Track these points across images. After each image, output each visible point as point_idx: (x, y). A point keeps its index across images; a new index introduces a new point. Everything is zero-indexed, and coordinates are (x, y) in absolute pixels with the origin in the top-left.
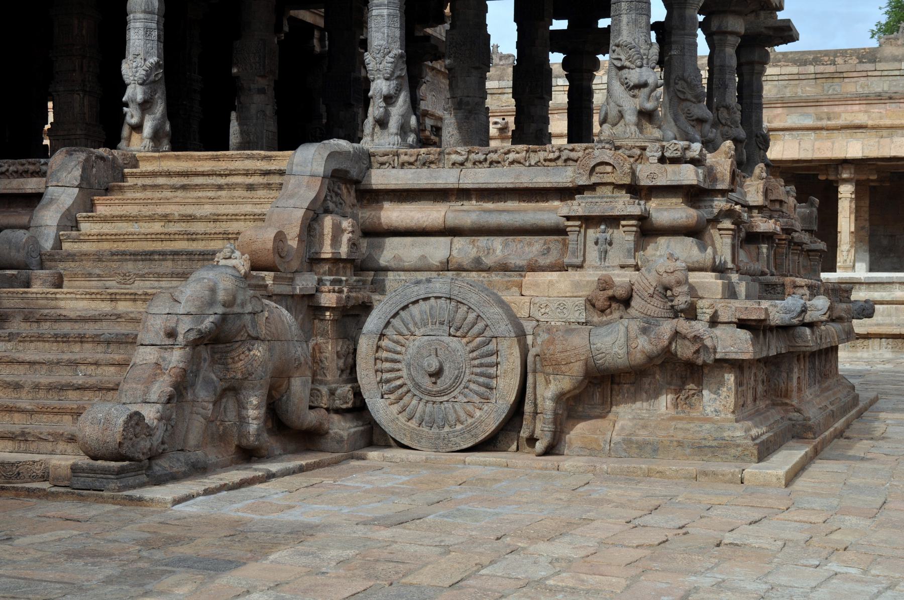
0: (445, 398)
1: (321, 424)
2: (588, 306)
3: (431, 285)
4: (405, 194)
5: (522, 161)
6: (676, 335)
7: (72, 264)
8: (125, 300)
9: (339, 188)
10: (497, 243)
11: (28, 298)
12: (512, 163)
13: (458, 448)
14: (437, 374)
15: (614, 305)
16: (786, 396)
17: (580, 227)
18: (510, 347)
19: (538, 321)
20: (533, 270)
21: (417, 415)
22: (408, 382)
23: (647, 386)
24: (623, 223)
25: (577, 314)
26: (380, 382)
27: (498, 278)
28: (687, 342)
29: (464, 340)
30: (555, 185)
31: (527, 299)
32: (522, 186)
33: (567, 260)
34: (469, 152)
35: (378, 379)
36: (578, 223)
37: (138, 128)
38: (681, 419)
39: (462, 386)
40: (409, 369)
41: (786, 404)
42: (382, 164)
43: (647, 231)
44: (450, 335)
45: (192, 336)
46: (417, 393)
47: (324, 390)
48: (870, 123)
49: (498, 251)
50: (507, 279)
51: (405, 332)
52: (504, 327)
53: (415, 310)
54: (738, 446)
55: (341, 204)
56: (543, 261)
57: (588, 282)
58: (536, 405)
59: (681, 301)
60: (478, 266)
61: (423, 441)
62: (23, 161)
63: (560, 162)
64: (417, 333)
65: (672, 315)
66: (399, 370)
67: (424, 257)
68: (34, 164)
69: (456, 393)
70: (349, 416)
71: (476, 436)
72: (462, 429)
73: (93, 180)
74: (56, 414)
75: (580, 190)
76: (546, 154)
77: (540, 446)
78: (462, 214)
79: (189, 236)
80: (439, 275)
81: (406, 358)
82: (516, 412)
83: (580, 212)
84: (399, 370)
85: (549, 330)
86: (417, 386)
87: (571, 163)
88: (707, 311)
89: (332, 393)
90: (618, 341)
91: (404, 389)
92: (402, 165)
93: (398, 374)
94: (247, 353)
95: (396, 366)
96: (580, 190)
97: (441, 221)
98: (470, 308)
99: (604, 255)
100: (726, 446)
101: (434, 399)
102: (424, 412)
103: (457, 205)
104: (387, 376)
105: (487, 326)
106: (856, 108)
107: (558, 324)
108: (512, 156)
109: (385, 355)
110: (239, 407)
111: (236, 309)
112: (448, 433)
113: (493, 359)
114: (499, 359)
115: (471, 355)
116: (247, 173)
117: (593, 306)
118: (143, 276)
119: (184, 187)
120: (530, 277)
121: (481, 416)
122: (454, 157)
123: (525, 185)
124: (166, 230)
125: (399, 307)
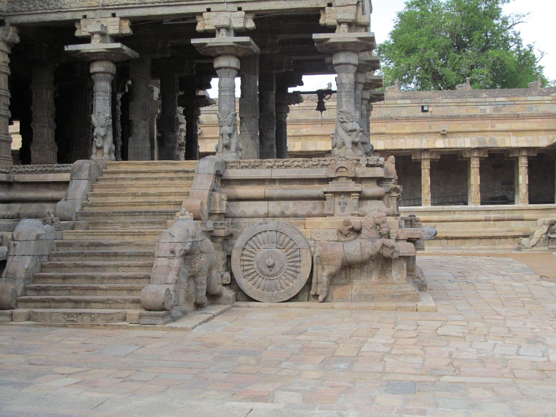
0: (276, 278)
1: (221, 291)
2: (339, 233)
3: (268, 225)
6: (384, 245)
7: (92, 218)
8: (129, 235)
10: (290, 203)
11: (78, 235)
12: (296, 167)
15: (351, 233)
16: (412, 271)
18: (306, 253)
20: (309, 217)
21: (262, 286)
22: (257, 270)
23: (366, 269)
24: (352, 194)
26: (243, 270)
27: (293, 221)
28: (388, 249)
29: (284, 250)
30: (318, 177)
31: (309, 230)
33: (326, 212)
34: (275, 161)
36: (331, 195)
37: (100, 148)
38: (383, 284)
41: (413, 275)
42: (232, 167)
43: (363, 198)
45: (182, 252)
46: (262, 275)
48: (387, 132)
49: (291, 208)
50: (298, 221)
51: (255, 247)
53: (259, 236)
54: (410, 295)
57: (337, 222)
58: (317, 279)
59: (384, 231)
60: (283, 215)
62: (45, 165)
63: (319, 166)
65: (379, 237)
67: (256, 211)
68: (50, 167)
69: (281, 275)
71: (290, 294)
74: (119, 290)
75: (331, 179)
77: (321, 298)
82: (309, 283)
83: (333, 190)
86: (262, 272)
87: (324, 166)
89: (222, 276)
90: (354, 249)
91: (255, 274)
92: (242, 167)
93: (252, 267)
95: (251, 263)
96: (331, 179)
97: (263, 194)
98: (287, 235)
99: (343, 209)
100: (405, 295)
101: (270, 278)
103: (270, 187)
104: (246, 268)
105: (295, 243)
106: (380, 124)
108: (296, 163)
109: (245, 258)
110: (196, 284)
111: (196, 239)
113: (298, 259)
115: (287, 257)
116: (167, 172)
117: (342, 233)
118: (133, 223)
120: (308, 220)
122: (268, 164)
124: (135, 201)
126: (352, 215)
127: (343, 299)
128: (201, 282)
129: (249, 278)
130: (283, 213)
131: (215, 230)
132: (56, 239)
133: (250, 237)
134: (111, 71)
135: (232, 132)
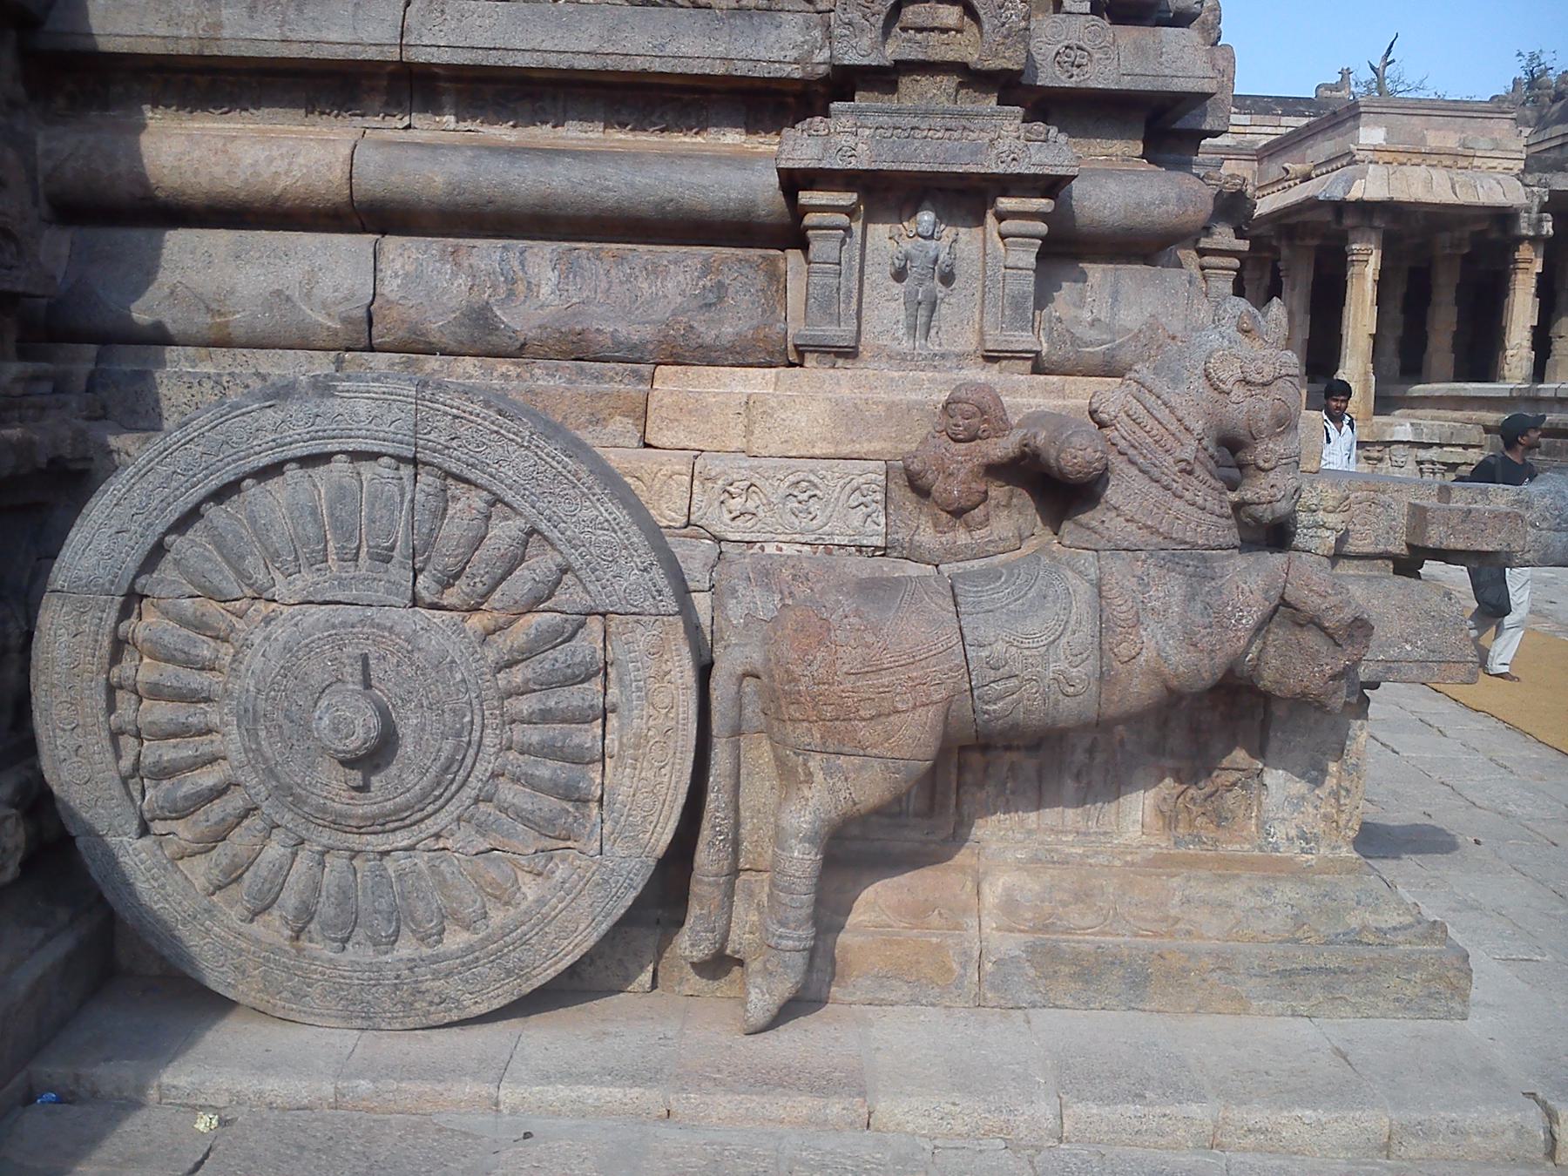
0: (402, 839)
2: (901, 493)
10: (541, 260)
14: (376, 755)
15: (998, 492)
17: (850, 212)
18: (657, 652)
19: (718, 540)
21: (290, 899)
24: (1005, 203)
25: (856, 518)
32: (625, 65)
36: (848, 198)
38: (1192, 863)
39: (468, 793)
40: (253, 734)
50: (589, 386)
52: (634, 577)
57: (890, 407)
61: (315, 991)
69: (443, 818)
72: (470, 949)
75: (844, 83)
78: (413, 153)
80: (339, 364)
81: (234, 686)
83: (863, 160)
85: (766, 575)
88: (1331, 519)
91: (234, 802)
93: (205, 746)
96: (844, 83)
98: (497, 500)
99: (924, 314)
101: (355, 841)
102: (316, 888)
103: (390, 127)
107: (788, 550)
120: (670, 383)
121: (541, 902)
123: (639, 64)
126: (991, 358)
127: (923, 979)
129: (184, 831)
130: (481, 318)
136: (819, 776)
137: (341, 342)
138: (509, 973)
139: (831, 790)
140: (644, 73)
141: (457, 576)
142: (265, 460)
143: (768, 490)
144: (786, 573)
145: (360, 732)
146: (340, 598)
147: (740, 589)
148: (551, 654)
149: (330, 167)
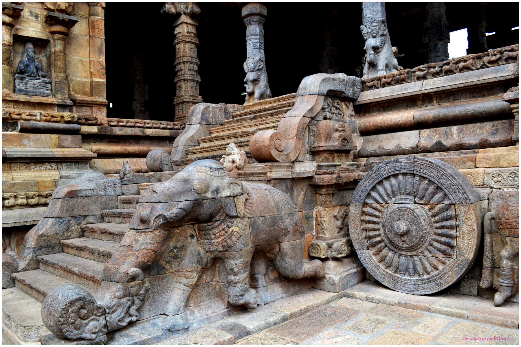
0: (414, 253)
3: (398, 164)
4: (387, 105)
5: (470, 66)
9: (338, 105)
10: (455, 129)
13: (427, 293)
19: (492, 188)
20: (484, 147)
22: (385, 239)
26: (365, 237)
29: (427, 207)
31: (481, 170)
34: (429, 68)
35: (364, 236)
37: (252, 94)
39: (427, 244)
40: (385, 230)
44: (415, 203)
46: (392, 248)
47: (323, 244)
49: (455, 136)
51: (381, 201)
53: (386, 184)
55: (340, 114)
56: (492, 139)
60: (439, 148)
64: (389, 202)
66: (379, 230)
67: (398, 146)
69: (422, 249)
70: (346, 260)
72: (429, 278)
73: (210, 120)
76: (488, 58)
77: (498, 297)
79: (240, 144)
84: (379, 230)
86: (391, 242)
87: (510, 61)
89: (330, 246)
94: (226, 229)
102: (399, 263)
109: (367, 218)
112: (417, 280)
113: (453, 222)
114: (457, 223)
115: (433, 219)
119: (254, 118)
120: (482, 153)
121: (444, 269)
122: (419, 73)
125: (375, 183)
128: (232, 270)
130: (439, 143)
131: (316, 176)
132: (123, 194)
133: (372, 185)
134: (258, 12)
135: (379, 44)
136: (509, 243)
137: (411, 152)
138: (437, 284)
139: (513, 246)
140: (475, 85)
141: (423, 197)
142: (386, 176)
143: (503, 175)
144: (508, 195)
145: (402, 229)
146: (400, 202)
147: (495, 200)
148: (443, 214)
149: (409, 117)
